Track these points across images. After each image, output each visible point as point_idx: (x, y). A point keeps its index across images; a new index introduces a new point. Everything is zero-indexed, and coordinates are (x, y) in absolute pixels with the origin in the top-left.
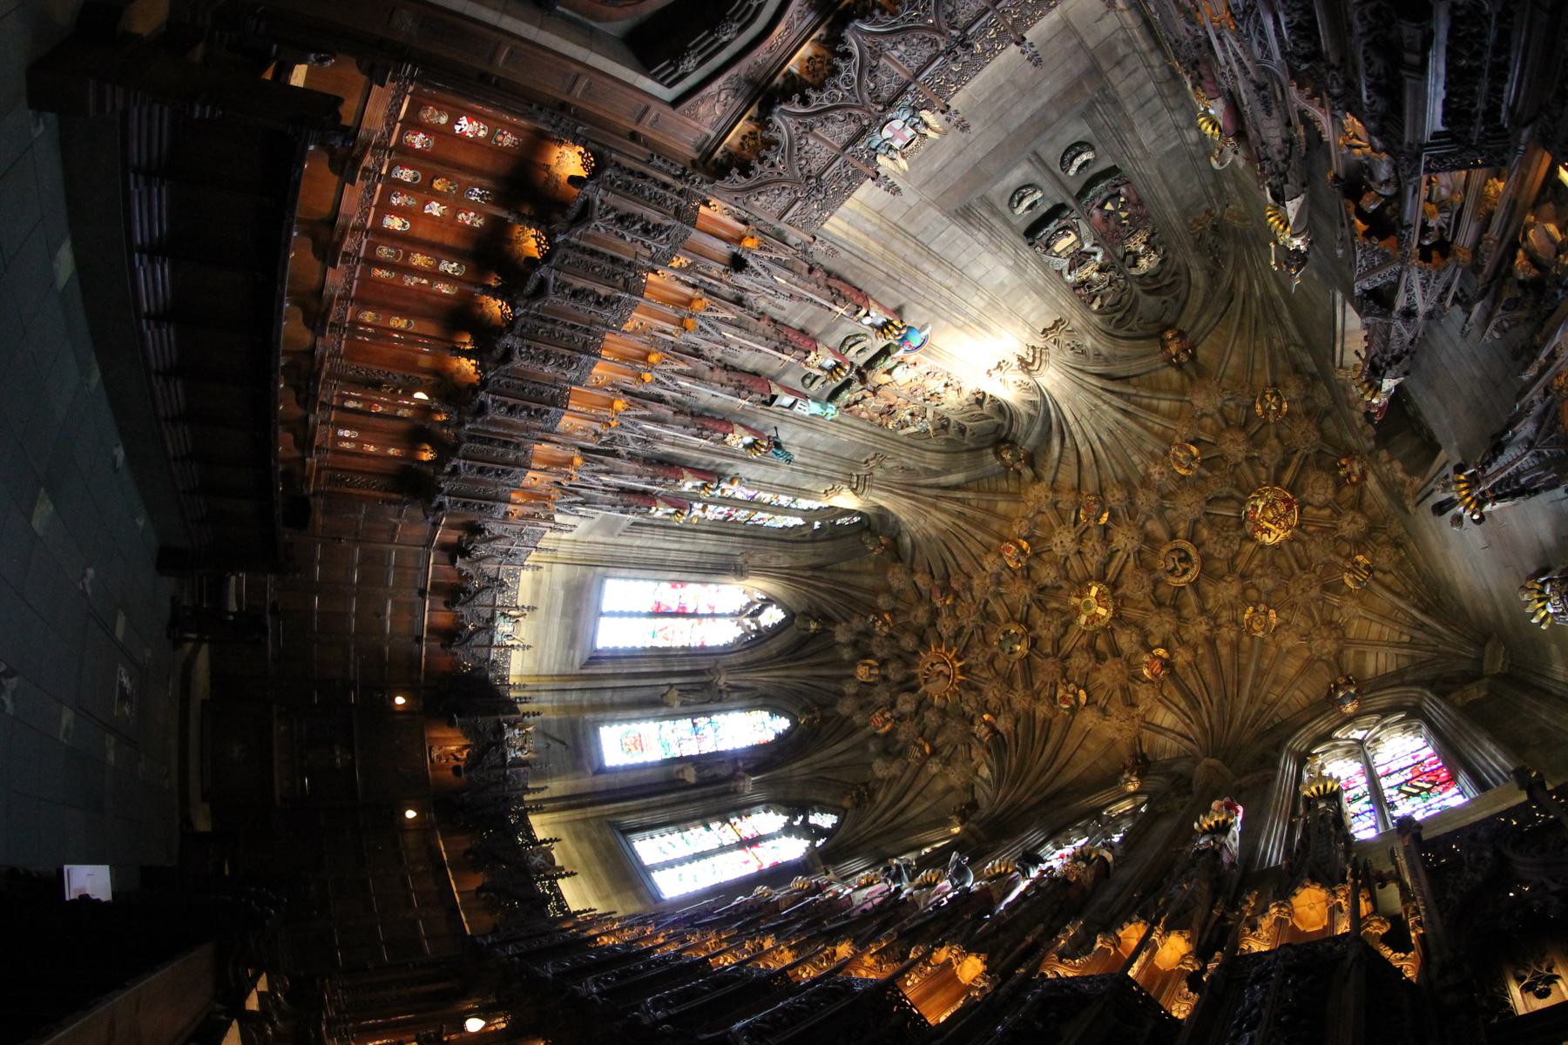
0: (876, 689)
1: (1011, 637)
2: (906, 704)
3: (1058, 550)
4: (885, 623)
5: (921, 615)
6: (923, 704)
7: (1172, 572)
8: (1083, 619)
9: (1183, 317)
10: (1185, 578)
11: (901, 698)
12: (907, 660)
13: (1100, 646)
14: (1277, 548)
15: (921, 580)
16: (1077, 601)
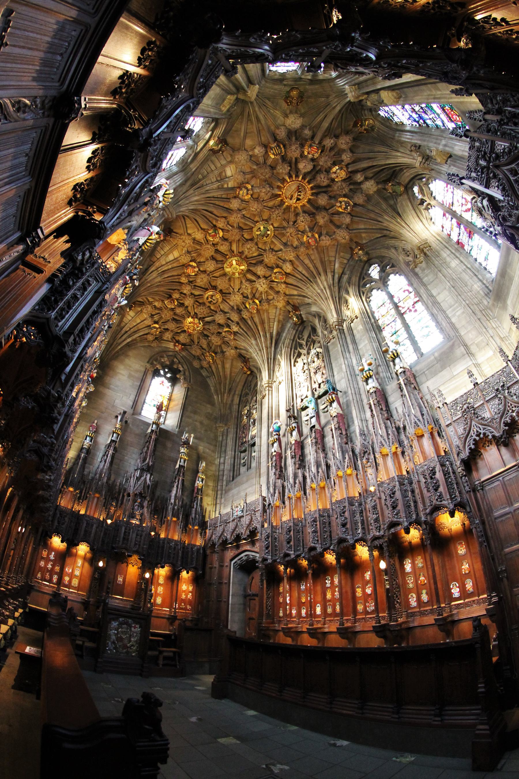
0: (329, 164)
1: (263, 236)
2: (304, 166)
3: (262, 281)
4: (341, 207)
5: (321, 219)
6: (294, 171)
7: (212, 296)
8: (234, 262)
9: (244, 380)
10: (207, 295)
11: (309, 167)
12: (318, 190)
13: (220, 258)
14: (184, 318)
15: (326, 241)
16: (243, 267)
